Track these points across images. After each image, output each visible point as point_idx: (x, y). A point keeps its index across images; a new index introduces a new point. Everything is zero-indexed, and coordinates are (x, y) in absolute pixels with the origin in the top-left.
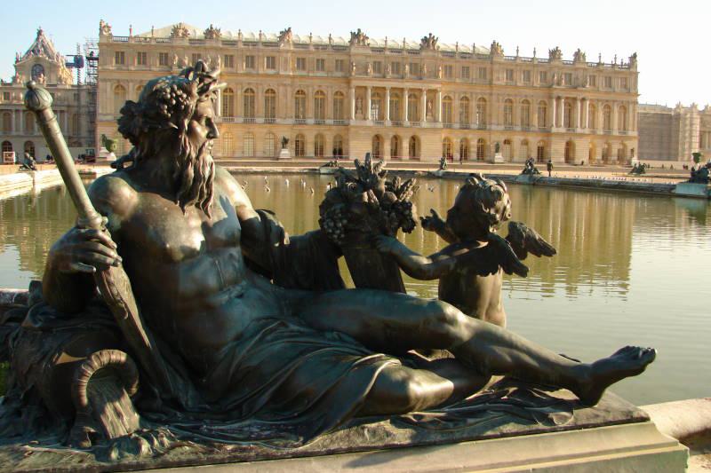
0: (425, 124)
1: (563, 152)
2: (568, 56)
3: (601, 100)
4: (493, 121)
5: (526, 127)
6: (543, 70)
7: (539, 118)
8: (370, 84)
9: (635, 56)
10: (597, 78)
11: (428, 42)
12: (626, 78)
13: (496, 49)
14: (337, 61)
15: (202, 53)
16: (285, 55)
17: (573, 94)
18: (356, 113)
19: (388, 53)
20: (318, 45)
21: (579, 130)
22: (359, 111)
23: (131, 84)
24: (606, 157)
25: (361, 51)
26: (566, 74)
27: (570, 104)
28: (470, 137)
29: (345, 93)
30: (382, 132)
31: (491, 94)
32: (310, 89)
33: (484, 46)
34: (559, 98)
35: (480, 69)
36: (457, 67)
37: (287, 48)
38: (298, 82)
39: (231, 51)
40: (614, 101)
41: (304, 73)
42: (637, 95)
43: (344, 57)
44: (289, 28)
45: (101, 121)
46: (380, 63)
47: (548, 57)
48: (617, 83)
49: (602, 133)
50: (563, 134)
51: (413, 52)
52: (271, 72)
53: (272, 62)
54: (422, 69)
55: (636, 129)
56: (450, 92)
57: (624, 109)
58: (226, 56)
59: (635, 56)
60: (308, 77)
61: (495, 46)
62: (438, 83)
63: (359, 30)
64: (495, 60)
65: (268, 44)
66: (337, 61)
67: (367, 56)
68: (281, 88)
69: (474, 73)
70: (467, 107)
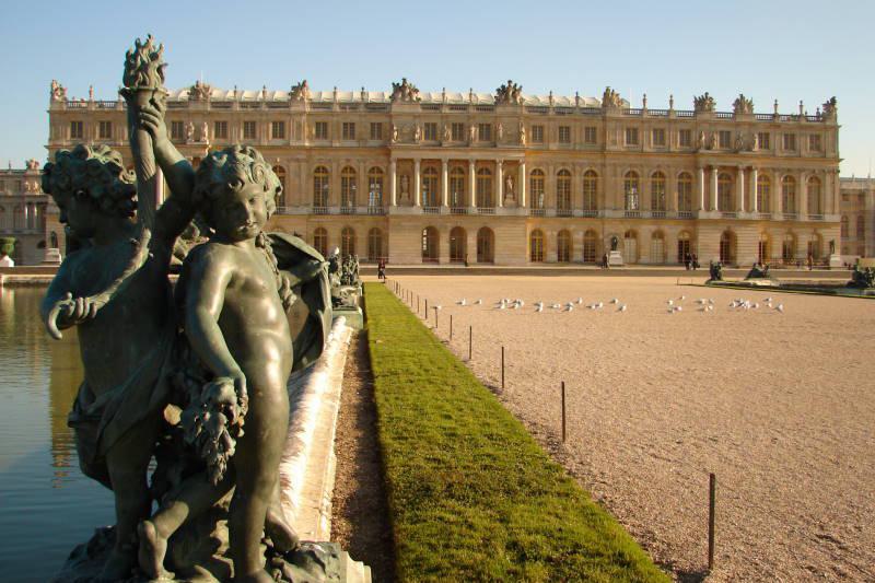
0: (500, 210)
1: (718, 247)
2: (724, 105)
3: (779, 170)
4: (609, 203)
5: (659, 209)
6: (686, 127)
7: (679, 197)
8: (417, 155)
9: (833, 101)
10: (771, 137)
11: (506, 93)
12: (818, 137)
13: (611, 100)
14: (373, 124)
15: (183, 119)
16: (297, 119)
17: (731, 162)
18: (505, 197)
19: (446, 110)
20: (345, 104)
21: (742, 215)
22: (405, 195)
24: (788, 254)
25: (407, 109)
26: (721, 133)
27: (729, 175)
28: (572, 228)
29: (384, 170)
30: (437, 224)
31: (604, 165)
32: (334, 165)
33: (592, 96)
34: (709, 169)
35: (587, 129)
36: (551, 129)
37: (300, 109)
38: (316, 156)
39: (223, 115)
40: (800, 171)
41: (325, 143)
43: (383, 119)
44: (304, 82)
45: (51, 214)
46: (434, 125)
47: (693, 109)
48: (804, 143)
49: (781, 218)
50: (715, 222)
51: (483, 108)
52: (279, 142)
53: (279, 130)
54: (497, 131)
55: (837, 210)
56: (541, 164)
57: (816, 181)
58: (217, 123)
59: (833, 101)
60: (331, 148)
62: (520, 151)
63: (404, 80)
64: (608, 115)
65: (274, 105)
66: (373, 124)
67: (415, 116)
68: (293, 166)
69: (578, 135)
70: (568, 184)
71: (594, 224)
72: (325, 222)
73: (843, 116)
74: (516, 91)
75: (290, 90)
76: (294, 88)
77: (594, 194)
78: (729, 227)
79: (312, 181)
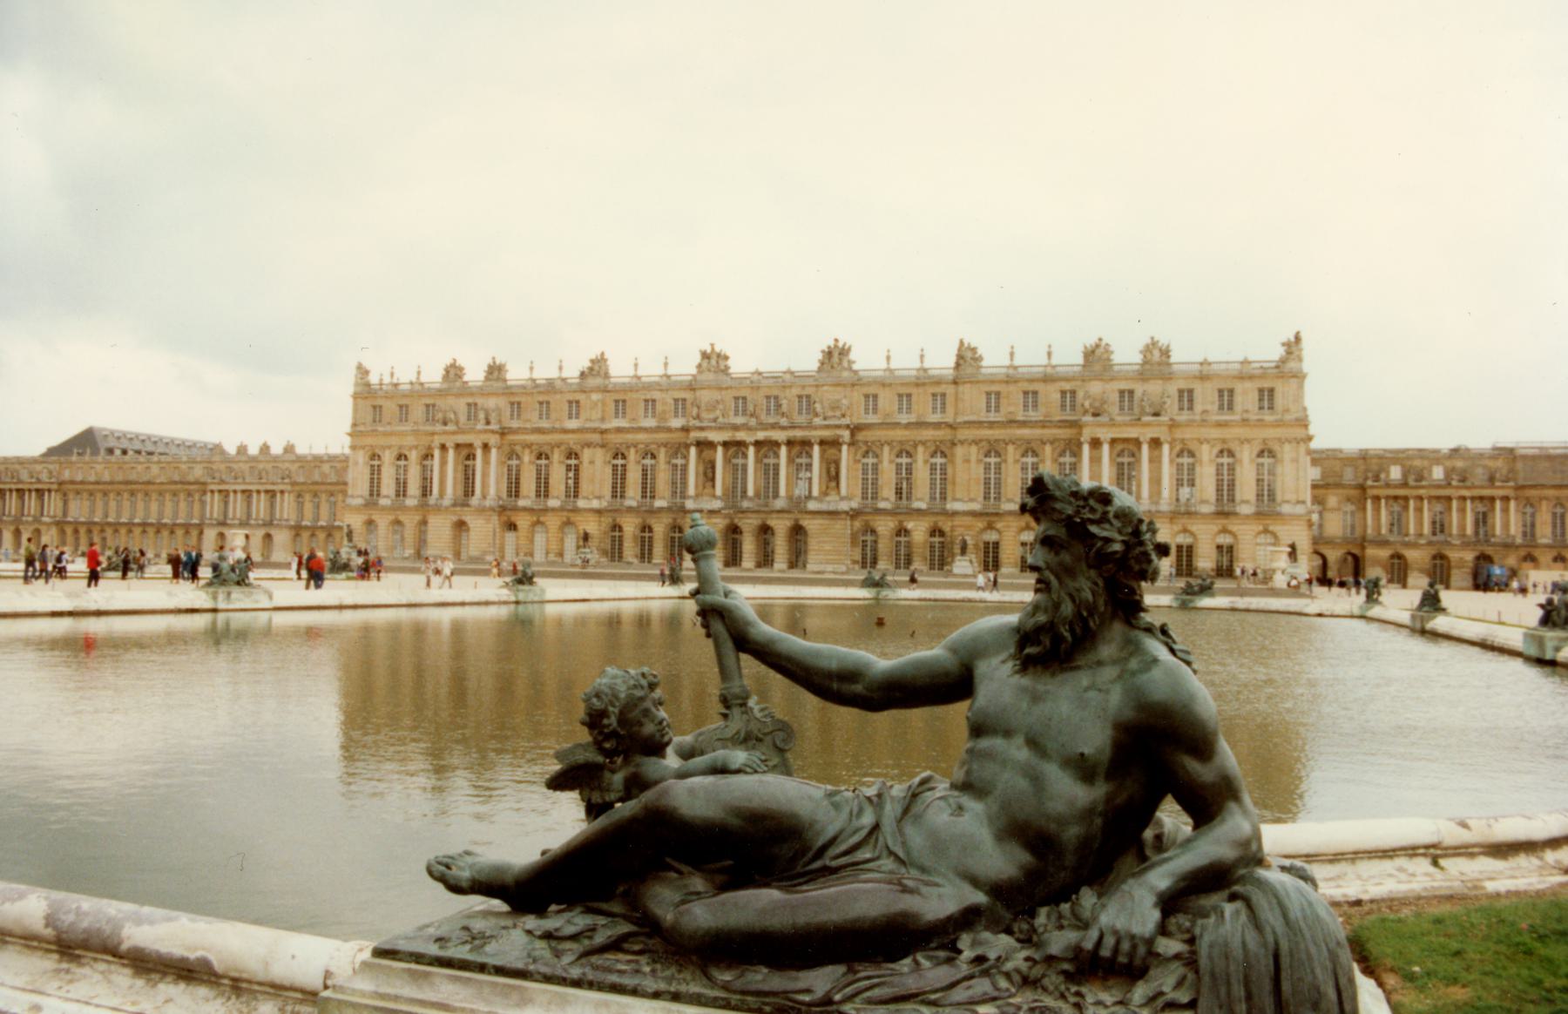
2: (1127, 354)
3: (1208, 441)
6: (1067, 386)
14: (676, 400)
17: (1132, 433)
23: (387, 453)
28: (910, 525)
42: (1303, 423)
61: (966, 357)
73: (1310, 362)
74: (844, 352)
76: (592, 361)
78: (901, 522)
79: (609, 470)
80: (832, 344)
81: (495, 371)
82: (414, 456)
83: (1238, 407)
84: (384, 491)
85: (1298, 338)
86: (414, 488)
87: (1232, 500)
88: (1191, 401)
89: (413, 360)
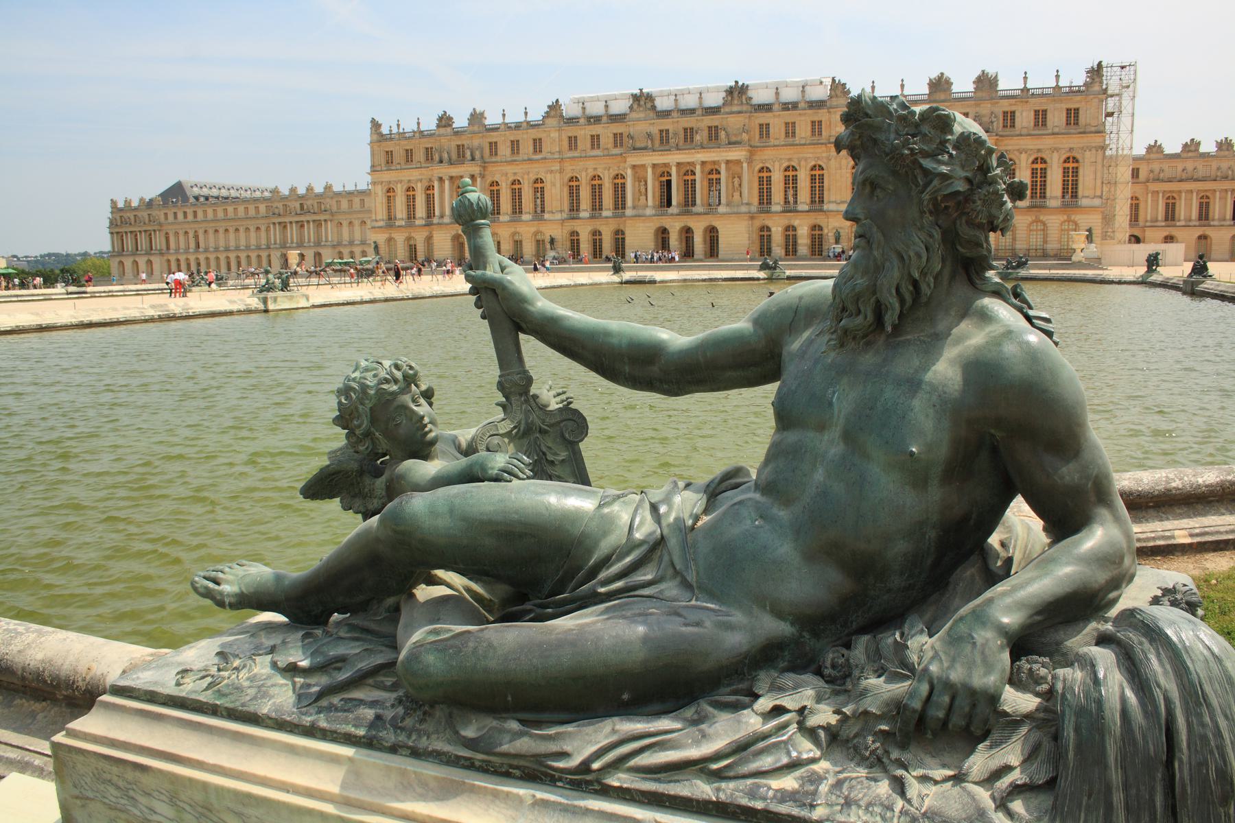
10: (1017, 114)
14: (615, 135)
28: (796, 223)
32: (584, 174)
35: (813, 122)
46: (667, 131)
65: (531, 125)
66: (615, 135)
70: (795, 179)
71: (820, 219)
72: (577, 226)
75: (546, 109)
76: (549, 107)
77: (822, 188)
80: (733, 84)
81: (476, 117)
82: (420, 188)
83: (1049, 123)
84: (399, 216)
85: (1100, 64)
86: (421, 211)
87: (1043, 196)
88: (1013, 120)
89: (414, 113)
